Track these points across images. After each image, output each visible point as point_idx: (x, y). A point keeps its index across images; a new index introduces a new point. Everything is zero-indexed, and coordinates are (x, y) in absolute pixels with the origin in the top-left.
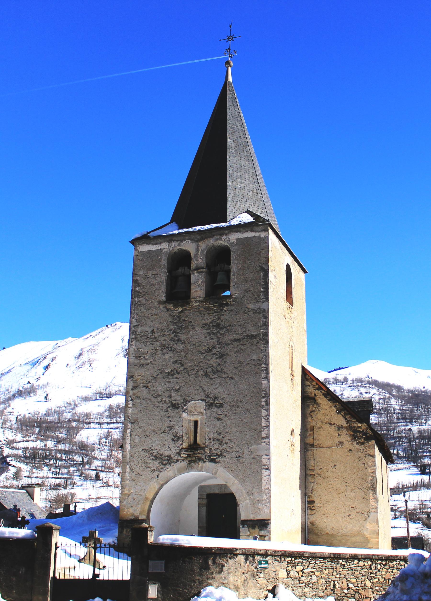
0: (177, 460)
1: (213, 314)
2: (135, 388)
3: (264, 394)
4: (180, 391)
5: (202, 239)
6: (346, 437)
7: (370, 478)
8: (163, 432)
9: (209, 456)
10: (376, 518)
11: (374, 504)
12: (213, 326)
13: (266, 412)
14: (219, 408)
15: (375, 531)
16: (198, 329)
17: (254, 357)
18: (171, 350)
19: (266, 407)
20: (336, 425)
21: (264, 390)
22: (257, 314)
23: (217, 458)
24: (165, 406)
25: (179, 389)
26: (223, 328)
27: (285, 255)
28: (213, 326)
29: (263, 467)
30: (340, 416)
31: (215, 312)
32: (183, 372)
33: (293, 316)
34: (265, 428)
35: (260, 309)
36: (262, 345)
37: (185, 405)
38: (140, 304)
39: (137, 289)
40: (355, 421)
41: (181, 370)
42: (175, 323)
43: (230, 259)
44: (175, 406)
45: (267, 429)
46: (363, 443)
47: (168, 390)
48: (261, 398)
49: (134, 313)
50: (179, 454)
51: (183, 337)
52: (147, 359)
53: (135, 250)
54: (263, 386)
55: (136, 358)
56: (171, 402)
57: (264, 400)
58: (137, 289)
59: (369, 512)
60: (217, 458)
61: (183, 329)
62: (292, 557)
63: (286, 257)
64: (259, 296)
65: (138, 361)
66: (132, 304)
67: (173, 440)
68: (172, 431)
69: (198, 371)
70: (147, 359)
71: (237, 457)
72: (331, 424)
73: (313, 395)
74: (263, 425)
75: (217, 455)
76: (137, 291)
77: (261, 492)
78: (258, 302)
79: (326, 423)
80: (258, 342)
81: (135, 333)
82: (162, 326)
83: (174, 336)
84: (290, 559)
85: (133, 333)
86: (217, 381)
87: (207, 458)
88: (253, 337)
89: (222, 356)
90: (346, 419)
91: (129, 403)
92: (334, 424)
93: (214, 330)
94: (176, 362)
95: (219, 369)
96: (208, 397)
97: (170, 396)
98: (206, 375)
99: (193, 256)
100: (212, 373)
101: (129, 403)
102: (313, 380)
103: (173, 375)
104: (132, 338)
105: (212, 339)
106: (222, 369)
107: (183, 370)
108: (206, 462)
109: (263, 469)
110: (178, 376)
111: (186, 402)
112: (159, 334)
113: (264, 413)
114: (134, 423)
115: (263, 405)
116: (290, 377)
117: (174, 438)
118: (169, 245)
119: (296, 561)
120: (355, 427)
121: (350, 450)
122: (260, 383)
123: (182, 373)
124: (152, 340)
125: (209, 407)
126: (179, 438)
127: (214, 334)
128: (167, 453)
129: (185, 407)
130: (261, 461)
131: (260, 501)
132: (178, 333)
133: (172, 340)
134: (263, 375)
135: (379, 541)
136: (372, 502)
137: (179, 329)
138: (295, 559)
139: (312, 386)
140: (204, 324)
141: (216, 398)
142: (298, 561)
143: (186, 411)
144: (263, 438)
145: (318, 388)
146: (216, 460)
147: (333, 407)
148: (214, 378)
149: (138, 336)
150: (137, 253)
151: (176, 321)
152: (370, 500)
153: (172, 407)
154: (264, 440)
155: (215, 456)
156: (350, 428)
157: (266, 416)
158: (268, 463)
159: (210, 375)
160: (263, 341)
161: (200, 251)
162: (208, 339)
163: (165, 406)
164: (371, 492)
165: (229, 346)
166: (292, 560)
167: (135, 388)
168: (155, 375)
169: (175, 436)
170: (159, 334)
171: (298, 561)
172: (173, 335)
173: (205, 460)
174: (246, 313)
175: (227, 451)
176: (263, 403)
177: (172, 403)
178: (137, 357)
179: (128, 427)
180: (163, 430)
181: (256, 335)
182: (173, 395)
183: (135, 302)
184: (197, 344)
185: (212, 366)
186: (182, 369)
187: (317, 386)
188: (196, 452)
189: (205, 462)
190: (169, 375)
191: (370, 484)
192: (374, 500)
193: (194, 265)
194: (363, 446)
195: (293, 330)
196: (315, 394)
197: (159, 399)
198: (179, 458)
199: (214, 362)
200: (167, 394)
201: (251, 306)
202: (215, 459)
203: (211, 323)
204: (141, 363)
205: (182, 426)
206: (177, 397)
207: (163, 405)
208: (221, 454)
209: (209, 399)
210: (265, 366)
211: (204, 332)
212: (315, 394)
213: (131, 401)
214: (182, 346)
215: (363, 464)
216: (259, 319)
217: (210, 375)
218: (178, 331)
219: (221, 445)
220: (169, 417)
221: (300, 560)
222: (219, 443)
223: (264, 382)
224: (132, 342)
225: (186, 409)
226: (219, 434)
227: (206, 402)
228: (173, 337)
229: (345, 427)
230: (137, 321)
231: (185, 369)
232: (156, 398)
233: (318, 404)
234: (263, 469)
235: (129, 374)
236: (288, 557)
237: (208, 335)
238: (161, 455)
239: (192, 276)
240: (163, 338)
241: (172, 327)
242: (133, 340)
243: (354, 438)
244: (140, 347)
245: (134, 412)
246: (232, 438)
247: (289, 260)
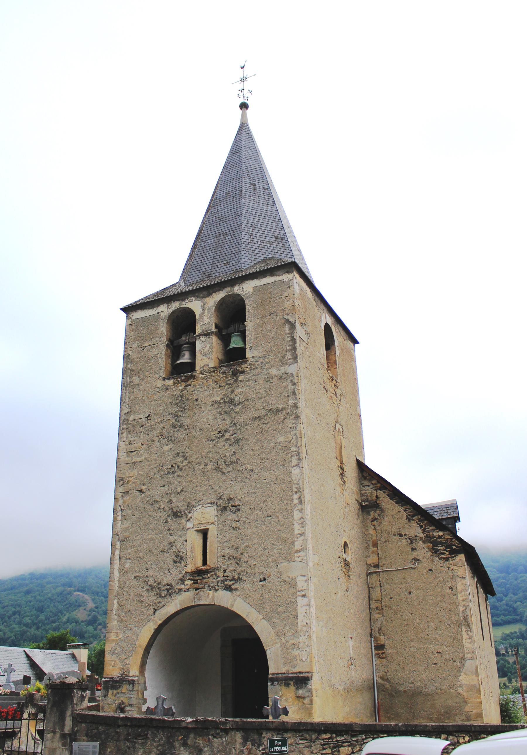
0: (179, 589)
1: (225, 386)
2: (126, 493)
3: (296, 488)
4: (183, 493)
5: (209, 295)
6: (423, 551)
7: (461, 609)
8: (162, 551)
9: (223, 582)
10: (474, 667)
11: (470, 646)
12: (225, 402)
13: (300, 514)
14: (234, 513)
15: (474, 686)
16: (207, 409)
17: (281, 439)
18: (171, 440)
19: (299, 507)
20: (407, 536)
21: (295, 482)
22: (283, 381)
23: (233, 584)
24: (164, 515)
25: (182, 491)
26: (238, 404)
27: (322, 311)
28: (225, 402)
29: (298, 593)
30: (414, 524)
31: (227, 384)
32: (187, 467)
33: (338, 392)
34: (299, 536)
35: (286, 373)
36: (291, 421)
37: (190, 512)
38: (132, 384)
39: (129, 366)
40: (434, 528)
41: (184, 466)
42: (176, 404)
43: (245, 314)
44: (176, 514)
45: (302, 538)
46: (447, 559)
47: (167, 494)
48: (293, 494)
49: (126, 396)
50: (182, 581)
51: (186, 422)
52: (142, 455)
53: (128, 318)
54: (294, 477)
55: (128, 456)
56: (172, 509)
57: (296, 496)
58: (129, 366)
59: (463, 659)
60: (233, 584)
61: (186, 411)
62: (332, 732)
63: (324, 314)
64: (284, 356)
65: (130, 459)
66: (123, 385)
67: (175, 562)
68: (174, 549)
69: (206, 465)
70: (142, 455)
71: (261, 581)
72: (401, 535)
73: (374, 497)
74: (297, 532)
75: (234, 579)
76: (129, 369)
77: (297, 631)
78: (283, 364)
79: (395, 535)
80: (285, 418)
81: (126, 422)
82: (160, 410)
83: (176, 421)
84: (328, 735)
85: (124, 422)
86: (233, 475)
87: (219, 584)
88: (279, 411)
89: (237, 441)
90: (421, 527)
91: (118, 514)
92: (405, 535)
93: (227, 408)
94: (178, 454)
95: (234, 459)
96: (220, 498)
97: (170, 502)
98: (218, 469)
99: (197, 317)
100: (224, 466)
101: (118, 514)
102: (373, 477)
103: (173, 472)
104: (123, 429)
105: (224, 420)
106: (238, 459)
107: (187, 465)
108: (218, 590)
109: (299, 596)
110: (180, 473)
111: (190, 507)
112: (156, 420)
113: (297, 515)
114: (124, 541)
115: (295, 504)
116: (338, 472)
117: (176, 559)
118: (168, 307)
119: (338, 739)
120: (435, 537)
121: (430, 570)
122: (290, 474)
123: (185, 469)
124: (147, 429)
125: (222, 511)
126: (182, 558)
127: (226, 412)
128: (167, 580)
129: (190, 515)
130: (294, 586)
131: (295, 646)
132: (180, 416)
133: (174, 426)
134: (294, 461)
135: (480, 703)
136: (467, 644)
137: (182, 411)
138: (337, 736)
139: (372, 486)
140: (213, 401)
141: (230, 499)
142: (343, 738)
143: (191, 520)
144: (297, 551)
145: (380, 487)
146: (233, 587)
147: (402, 511)
148: (228, 472)
149: (131, 426)
150: (130, 323)
151: (177, 401)
152: (464, 641)
153: (173, 516)
154: (299, 554)
155: (231, 581)
156: (428, 539)
157: (300, 519)
158: (305, 587)
159: (222, 469)
160: (292, 416)
161: (206, 310)
162: (219, 420)
163: (164, 515)
164: (464, 628)
165: (247, 427)
166: (331, 738)
167: (126, 493)
168: (151, 475)
169: (177, 556)
170: (156, 420)
171: (343, 738)
172: (173, 420)
173: (217, 588)
174: (268, 381)
175: (247, 573)
176: (296, 501)
177: (173, 511)
178: (129, 452)
179: (117, 547)
180: (161, 549)
181: (282, 409)
182: (174, 500)
183: (127, 382)
184: (205, 429)
185: (225, 456)
186: (185, 463)
187: (379, 485)
188: (205, 576)
189: (217, 590)
190: (169, 473)
191: (462, 618)
192: (469, 641)
193: (199, 329)
194: (447, 563)
195: (340, 410)
196: (377, 497)
197: (157, 505)
198: (182, 586)
199: (228, 450)
200: (166, 500)
201: (274, 371)
202: (230, 586)
203: (222, 399)
204: (133, 461)
205: (186, 541)
206: (179, 503)
207: (161, 514)
208: (239, 577)
209: (221, 501)
210: (295, 449)
211: (214, 412)
212: (377, 497)
213: (121, 512)
214: (185, 432)
215: (450, 588)
216: (286, 387)
217: (222, 469)
218: (180, 414)
219: (238, 564)
220: (169, 530)
221: (345, 737)
222: (236, 562)
223: (296, 472)
224: (122, 433)
225: (191, 517)
226: (236, 549)
227: (218, 506)
228: (173, 423)
229: (421, 539)
230: (129, 406)
231: (189, 462)
232: (152, 505)
233: (382, 511)
234: (299, 596)
235: (119, 476)
236: (325, 732)
237: (218, 416)
238: (159, 584)
239: (198, 343)
240: (161, 426)
241: (171, 410)
242: (123, 431)
243: (435, 552)
244: (133, 439)
245: (124, 526)
246: (254, 554)
247: (330, 321)
